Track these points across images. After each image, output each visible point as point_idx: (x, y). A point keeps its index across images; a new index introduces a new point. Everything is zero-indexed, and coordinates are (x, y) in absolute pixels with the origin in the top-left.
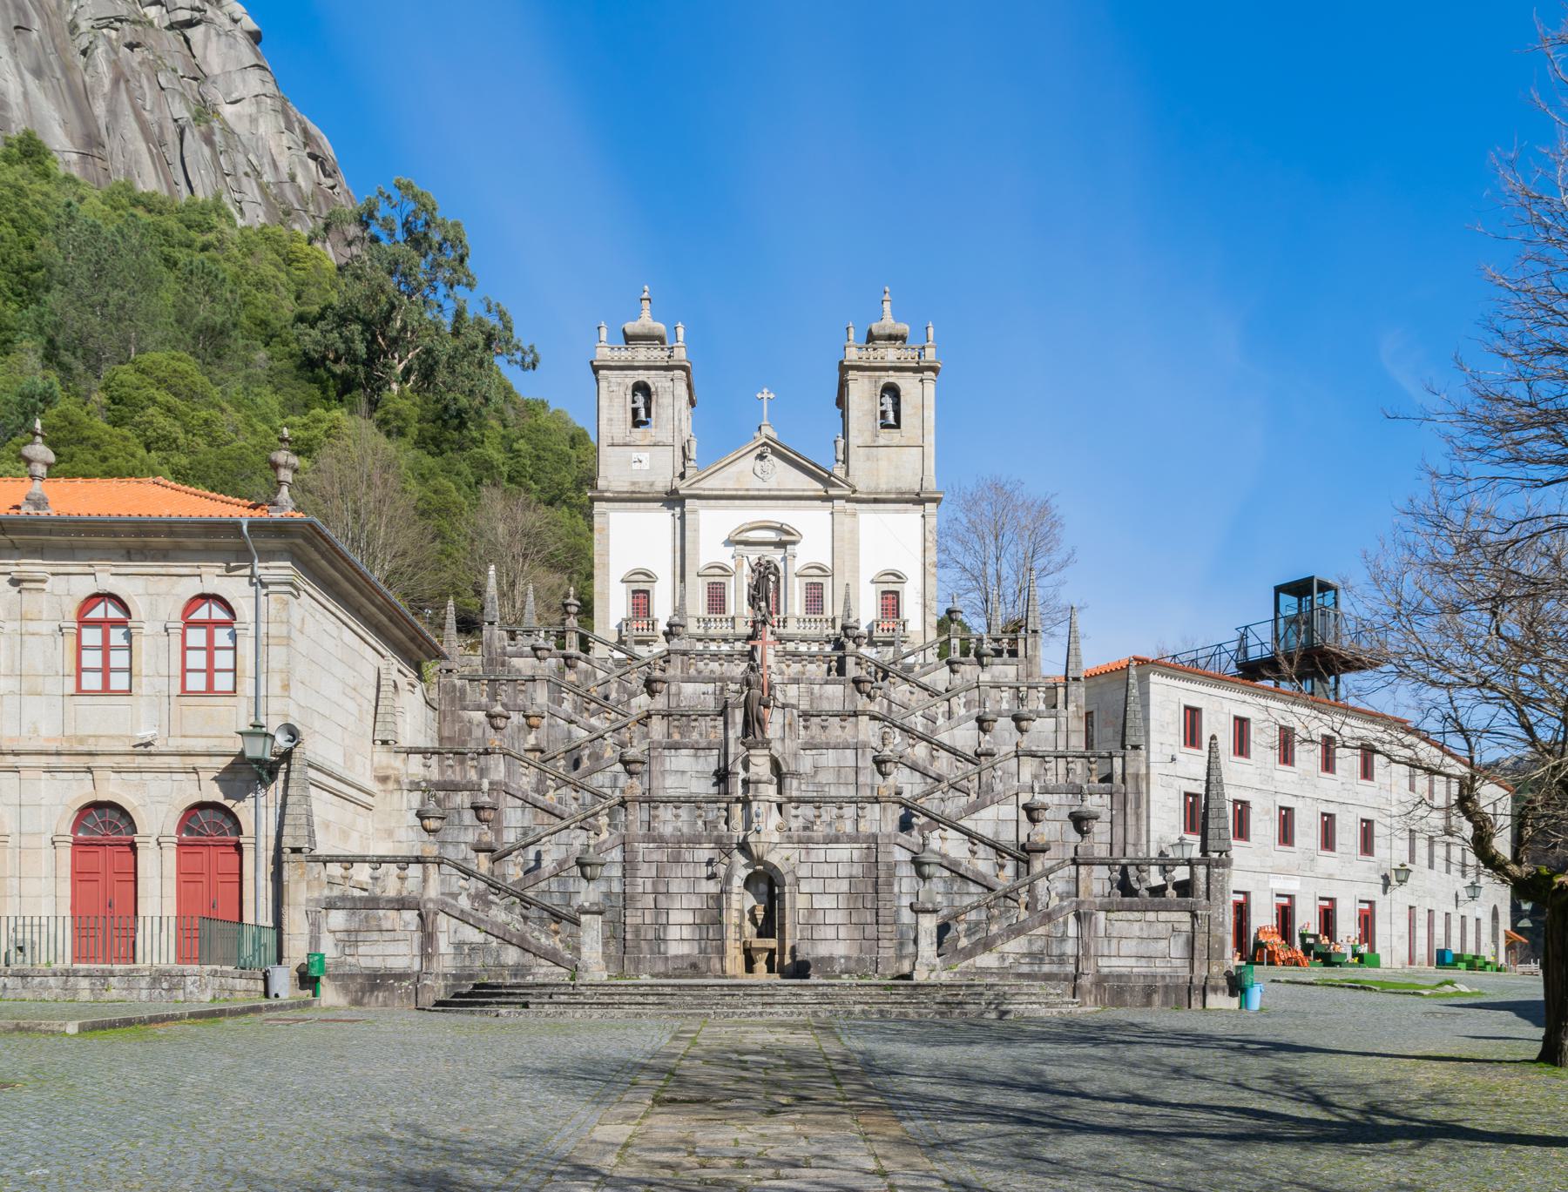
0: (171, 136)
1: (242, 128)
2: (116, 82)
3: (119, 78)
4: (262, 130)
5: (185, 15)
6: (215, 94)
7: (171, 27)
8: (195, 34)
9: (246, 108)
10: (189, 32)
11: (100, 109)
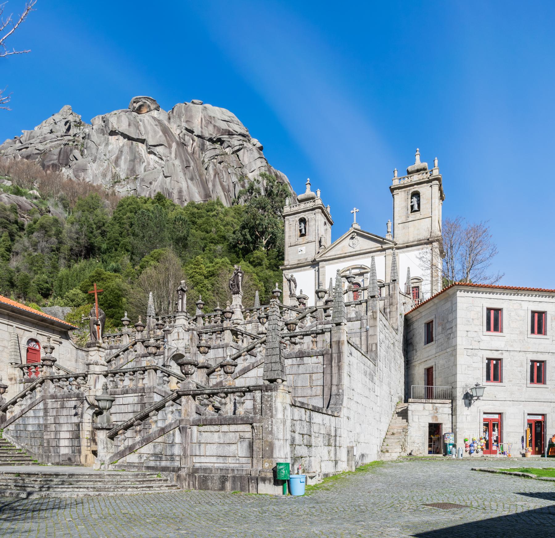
2: (215, 176)
3: (216, 173)
5: (237, 148)
6: (246, 171)
7: (233, 153)
8: (240, 153)
10: (238, 153)
11: (210, 185)
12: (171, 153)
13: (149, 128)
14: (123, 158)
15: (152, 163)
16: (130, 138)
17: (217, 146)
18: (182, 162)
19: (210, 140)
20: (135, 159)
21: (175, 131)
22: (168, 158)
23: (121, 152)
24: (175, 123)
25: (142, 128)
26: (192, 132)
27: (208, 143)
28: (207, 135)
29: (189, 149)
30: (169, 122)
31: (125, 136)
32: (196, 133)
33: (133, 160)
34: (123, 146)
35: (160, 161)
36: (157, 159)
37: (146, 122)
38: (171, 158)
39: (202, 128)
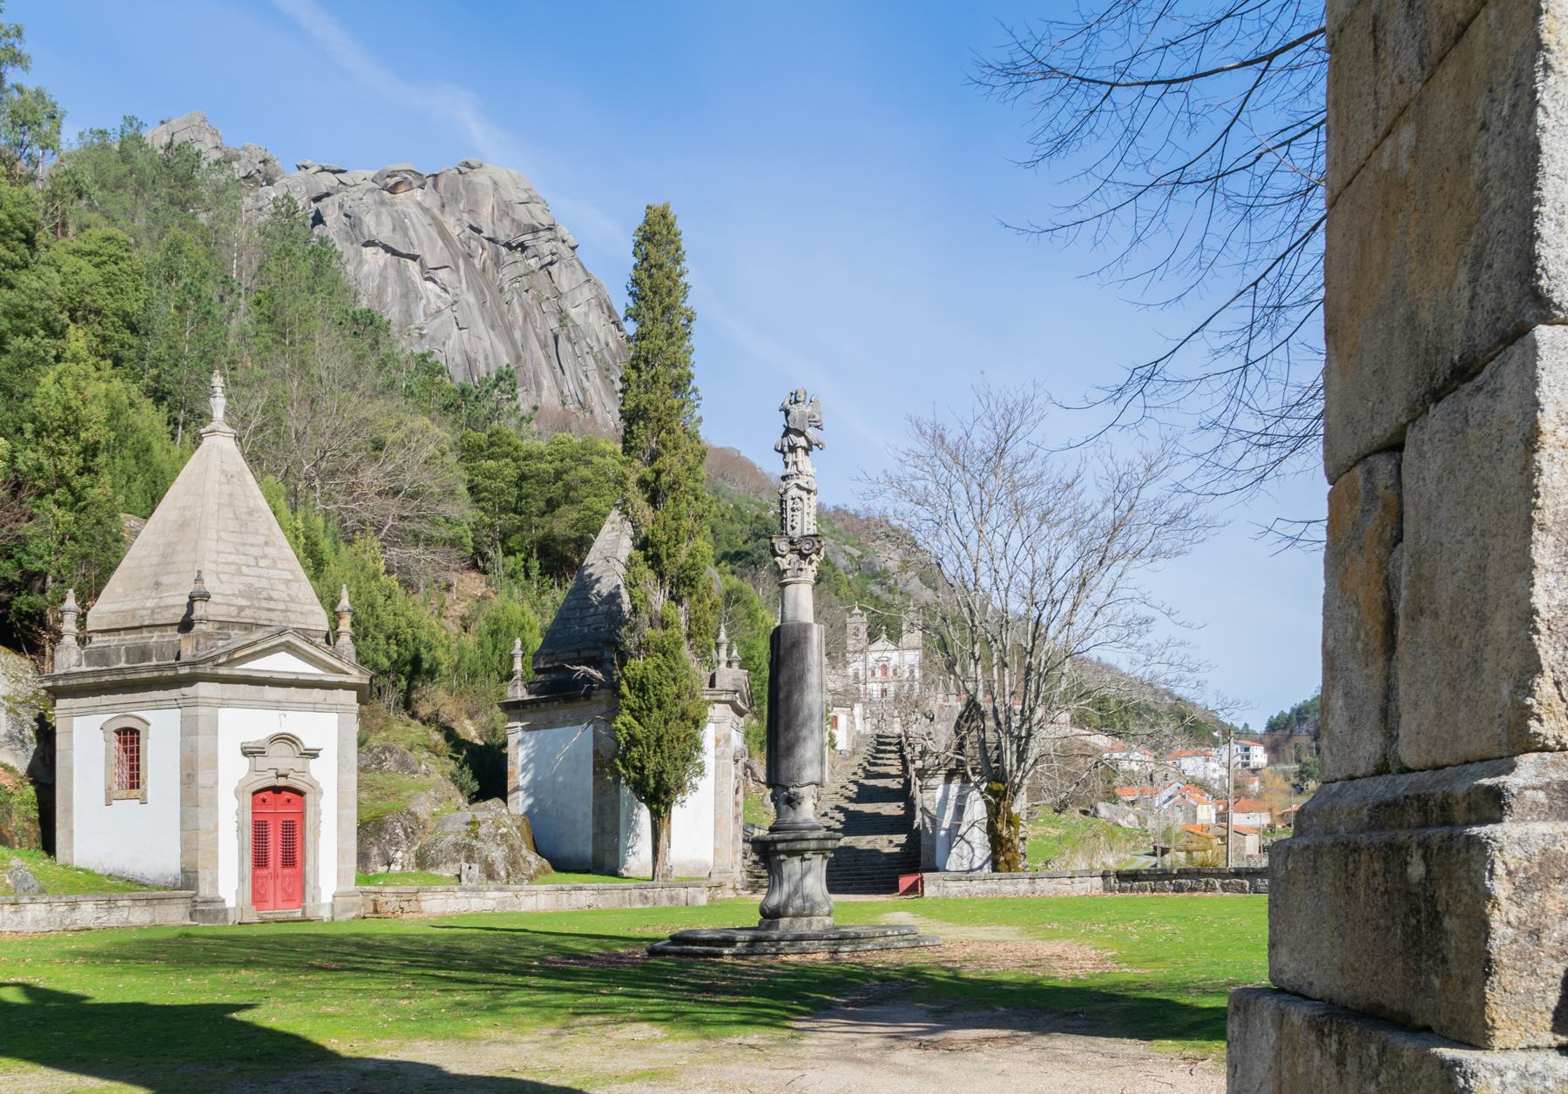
0: (551, 341)
1: (580, 321)
2: (525, 318)
3: (526, 316)
4: (591, 320)
5: (548, 259)
6: (566, 304)
7: (541, 268)
9: (583, 309)
10: (551, 268)
11: (517, 335)
12: (460, 282)
13: (421, 231)
15: (433, 299)
16: (394, 253)
17: (518, 255)
18: (476, 296)
19: (508, 245)
20: (409, 293)
21: (454, 230)
23: (384, 278)
24: (452, 214)
25: (411, 233)
26: (479, 231)
27: (504, 250)
28: (502, 238)
29: (477, 263)
30: (442, 212)
31: (387, 249)
32: (485, 234)
33: (405, 295)
34: (385, 264)
35: (443, 294)
36: (438, 290)
38: (462, 291)
39: (493, 223)
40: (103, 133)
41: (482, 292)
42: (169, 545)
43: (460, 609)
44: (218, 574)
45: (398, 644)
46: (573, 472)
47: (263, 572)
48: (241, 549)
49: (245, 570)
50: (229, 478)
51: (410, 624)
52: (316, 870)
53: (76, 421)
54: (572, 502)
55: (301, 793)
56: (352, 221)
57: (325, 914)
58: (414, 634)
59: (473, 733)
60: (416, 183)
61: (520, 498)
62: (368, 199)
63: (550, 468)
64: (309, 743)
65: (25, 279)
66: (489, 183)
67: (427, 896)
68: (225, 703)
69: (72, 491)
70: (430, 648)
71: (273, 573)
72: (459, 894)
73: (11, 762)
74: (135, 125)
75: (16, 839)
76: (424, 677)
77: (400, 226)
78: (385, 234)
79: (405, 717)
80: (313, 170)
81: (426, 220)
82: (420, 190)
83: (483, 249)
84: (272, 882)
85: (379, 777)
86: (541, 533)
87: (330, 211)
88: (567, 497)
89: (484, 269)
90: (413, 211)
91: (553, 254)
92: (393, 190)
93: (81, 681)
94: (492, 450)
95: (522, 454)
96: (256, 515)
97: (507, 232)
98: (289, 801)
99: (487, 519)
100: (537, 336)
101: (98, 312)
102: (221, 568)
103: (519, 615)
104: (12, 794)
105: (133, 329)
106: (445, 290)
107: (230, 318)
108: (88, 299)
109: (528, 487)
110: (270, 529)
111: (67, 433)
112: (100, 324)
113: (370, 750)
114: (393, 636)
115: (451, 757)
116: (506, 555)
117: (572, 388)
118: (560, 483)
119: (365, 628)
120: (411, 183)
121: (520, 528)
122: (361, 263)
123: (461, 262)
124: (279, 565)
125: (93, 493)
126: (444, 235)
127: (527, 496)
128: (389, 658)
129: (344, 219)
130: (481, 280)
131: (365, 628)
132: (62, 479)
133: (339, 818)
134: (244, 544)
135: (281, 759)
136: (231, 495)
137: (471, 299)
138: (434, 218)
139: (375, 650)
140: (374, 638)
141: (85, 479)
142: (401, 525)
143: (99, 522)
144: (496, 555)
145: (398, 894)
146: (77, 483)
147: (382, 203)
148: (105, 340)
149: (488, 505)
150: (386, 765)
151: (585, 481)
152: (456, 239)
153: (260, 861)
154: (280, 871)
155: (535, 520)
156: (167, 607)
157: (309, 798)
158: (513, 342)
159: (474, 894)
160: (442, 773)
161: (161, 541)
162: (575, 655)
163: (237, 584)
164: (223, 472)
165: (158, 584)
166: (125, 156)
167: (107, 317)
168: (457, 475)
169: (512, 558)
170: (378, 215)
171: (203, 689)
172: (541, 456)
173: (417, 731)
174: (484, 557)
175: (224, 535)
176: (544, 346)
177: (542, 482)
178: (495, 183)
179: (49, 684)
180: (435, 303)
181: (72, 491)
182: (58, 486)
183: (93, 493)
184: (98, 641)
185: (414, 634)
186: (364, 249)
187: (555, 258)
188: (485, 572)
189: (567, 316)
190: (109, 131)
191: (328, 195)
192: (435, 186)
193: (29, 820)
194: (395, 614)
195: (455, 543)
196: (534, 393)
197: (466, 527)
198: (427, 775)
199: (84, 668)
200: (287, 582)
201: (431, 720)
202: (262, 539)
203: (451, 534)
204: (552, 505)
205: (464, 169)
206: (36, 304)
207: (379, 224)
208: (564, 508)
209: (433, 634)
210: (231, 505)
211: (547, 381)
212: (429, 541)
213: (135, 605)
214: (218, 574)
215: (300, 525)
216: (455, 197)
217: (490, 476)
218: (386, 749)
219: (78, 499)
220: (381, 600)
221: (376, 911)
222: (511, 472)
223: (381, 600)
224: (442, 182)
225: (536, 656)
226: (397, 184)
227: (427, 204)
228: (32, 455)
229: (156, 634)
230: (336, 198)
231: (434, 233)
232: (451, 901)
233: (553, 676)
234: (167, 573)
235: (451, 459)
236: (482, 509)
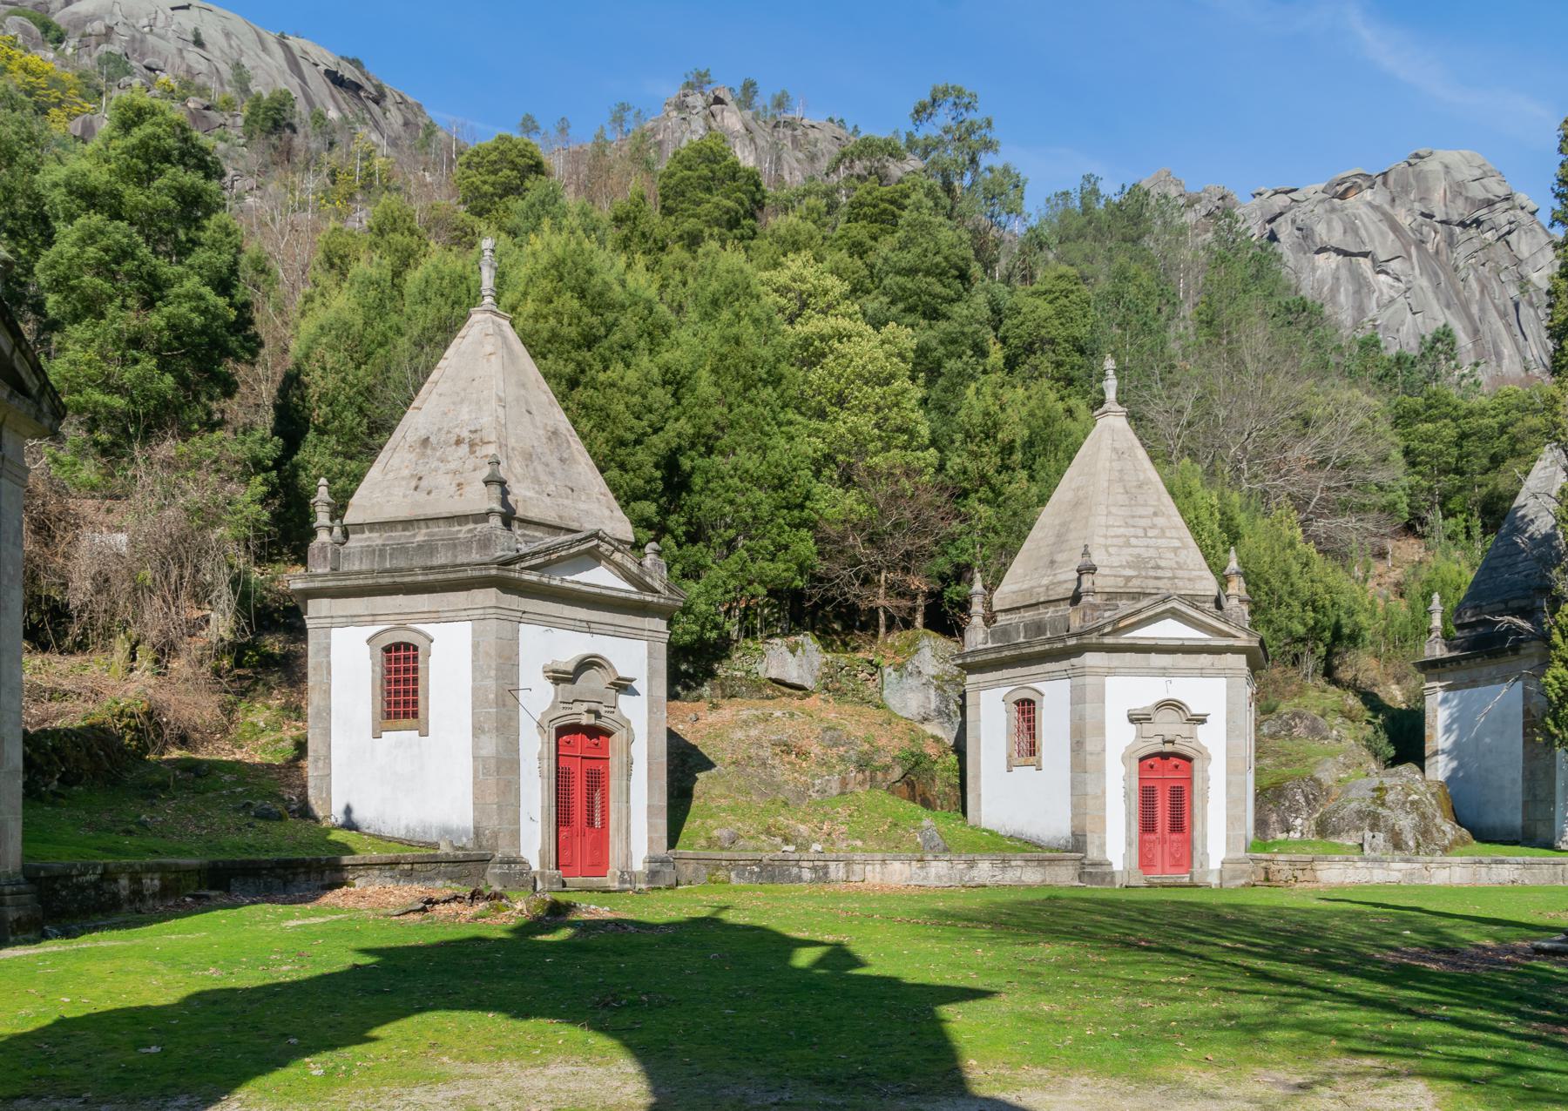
0: (1511, 310)
2: (1482, 292)
3: (1483, 288)
5: (1506, 229)
6: (1527, 270)
8: (1512, 238)
10: (1509, 238)
11: (1475, 309)
12: (1413, 269)
13: (1372, 229)
14: (1342, 289)
15: (1385, 290)
16: (1346, 254)
17: (1473, 231)
18: (1430, 280)
19: (1462, 224)
20: (1361, 286)
21: (1404, 219)
22: (1411, 278)
24: (1403, 205)
25: (1363, 233)
26: (1431, 216)
27: (1458, 230)
29: (1430, 247)
31: (1339, 251)
32: (1438, 218)
35: (1396, 284)
36: (1390, 280)
37: (1364, 216)
38: (1415, 277)
39: (1446, 205)
40: (1066, 194)
41: (1436, 274)
42: (1063, 524)
43: (1396, 575)
44: (1106, 547)
45: (1315, 610)
46: (1520, 423)
47: (1152, 542)
48: (1130, 521)
49: (1133, 541)
50: (1120, 454)
51: (1329, 590)
52: (1205, 836)
53: (995, 424)
54: (1519, 455)
55: (1189, 759)
56: (1305, 232)
57: (1214, 880)
58: (1332, 600)
59: (1400, 698)
60: (1365, 185)
61: (1460, 458)
62: (1319, 210)
63: (1494, 423)
64: (1196, 709)
65: (959, 310)
66: (1440, 168)
67: (1325, 865)
68: (1111, 672)
69: (993, 489)
70: (1351, 613)
71: (1160, 542)
72: (1360, 864)
73: (939, 733)
74: (1092, 180)
75: (938, 802)
76: (1345, 642)
77: (1351, 228)
78: (1337, 238)
79: (1321, 682)
80: (1266, 195)
81: (1376, 217)
82: (1369, 191)
83: (1436, 232)
84: (1159, 847)
85: (1288, 743)
86: (1484, 491)
87: (1285, 230)
88: (1513, 450)
89: (1437, 252)
90: (1364, 211)
91: (1511, 223)
92: (1343, 196)
93: (985, 657)
94: (1430, 412)
95: (1462, 413)
96: (1146, 487)
97: (1461, 211)
98: (1177, 767)
99: (1425, 484)
100: (1496, 306)
101: (1052, 342)
102: (1109, 542)
103: (1454, 575)
104: (936, 762)
105: (1082, 351)
106: (1398, 280)
107: (1167, 326)
108: (1043, 332)
109: (1468, 446)
110: (1159, 499)
111: (988, 437)
112: (1054, 351)
113: (1280, 717)
114: (1313, 604)
115: (1369, 722)
116: (1445, 518)
117: (1535, 352)
118: (1505, 437)
119: (1280, 597)
120: (1360, 186)
121: (1461, 489)
122: (1314, 269)
123: (1413, 250)
124: (1168, 534)
125: (1008, 489)
126: (1395, 227)
127: (1469, 455)
128: (1305, 625)
129: (1297, 233)
130: (1437, 267)
131: (1280, 597)
132: (984, 478)
133: (1228, 784)
134: (1133, 517)
135: (1168, 725)
136: (1121, 471)
137: (1424, 282)
138: (1384, 214)
139: (1290, 618)
140: (1288, 605)
141: (1004, 477)
142: (1333, 495)
143: (1015, 514)
144: (1435, 517)
145: (1291, 862)
146: (997, 480)
147: (1333, 210)
148: (1059, 365)
149: (1426, 469)
150: (1296, 732)
151: (1533, 431)
152: (1407, 228)
153: (1148, 825)
154: (1167, 836)
155: (1478, 478)
156: (1060, 583)
157: (1197, 764)
158: (1470, 317)
159: (1377, 865)
160: (1356, 739)
161: (1057, 522)
162: (1502, 606)
163: (1126, 555)
164: (1115, 450)
165: (1052, 562)
166: (1086, 210)
167: (1059, 344)
168: (1392, 442)
169: (1452, 521)
170: (1329, 223)
171: (1090, 659)
172: (1483, 412)
173: (1334, 695)
174: (1423, 521)
175: (1114, 510)
176: (1503, 315)
177: (1484, 437)
178: (1446, 167)
179: (960, 661)
180: (1388, 293)
181: (993, 489)
182: (981, 485)
183: (1008, 489)
184: (1002, 619)
185: (1332, 600)
186: (1316, 256)
187: (1513, 226)
188: (1423, 536)
189: (1529, 281)
190: (1071, 191)
191: (1281, 214)
192: (1385, 183)
193: (950, 785)
194: (1312, 581)
195: (1390, 509)
196: (1494, 364)
197: (1401, 492)
198: (1339, 741)
199: (990, 645)
200: (1175, 550)
201: (1353, 686)
202: (1152, 510)
203: (1384, 502)
204: (1496, 461)
205: (1413, 161)
206: (966, 330)
207: (1330, 228)
208: (1510, 462)
209: (1355, 600)
210: (1121, 480)
211: (1507, 350)
212: (1363, 508)
213: (1033, 583)
214: (1106, 547)
215: (1215, 501)
216: (1405, 190)
217: (1428, 439)
218: (1296, 715)
219: (998, 494)
220: (1296, 568)
221: (1267, 879)
222: (1450, 432)
223: (1296, 568)
224: (1391, 178)
225: (1459, 611)
226: (1347, 190)
227: (1377, 202)
228: (958, 460)
229: (1051, 609)
230: (1289, 216)
231: (1385, 227)
232: (1351, 871)
233: (1481, 630)
234: (1061, 551)
235: (1384, 427)
236: (1419, 473)
